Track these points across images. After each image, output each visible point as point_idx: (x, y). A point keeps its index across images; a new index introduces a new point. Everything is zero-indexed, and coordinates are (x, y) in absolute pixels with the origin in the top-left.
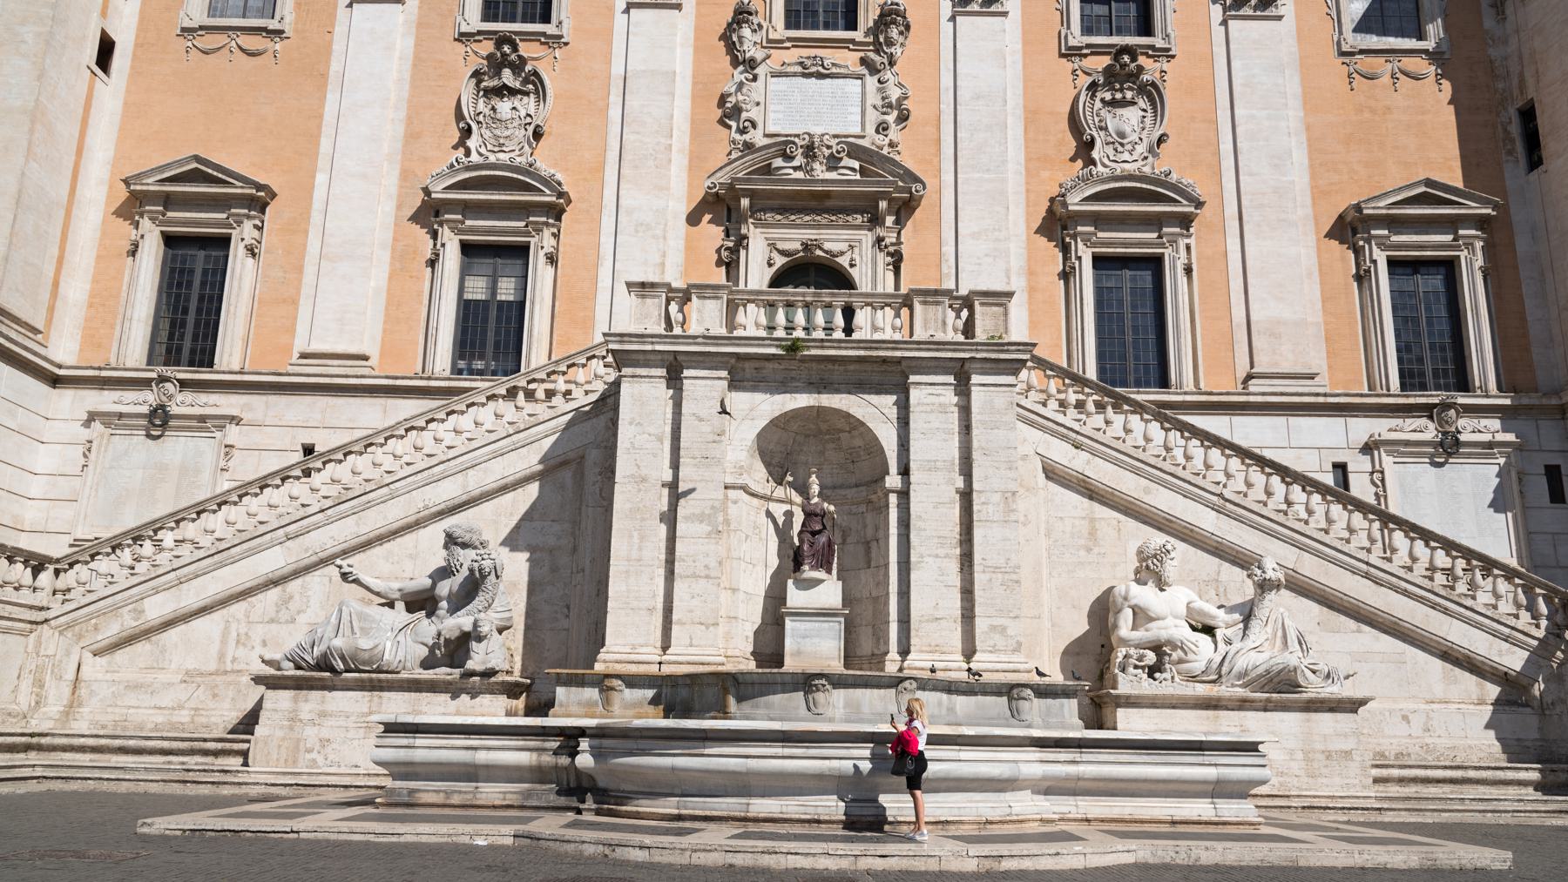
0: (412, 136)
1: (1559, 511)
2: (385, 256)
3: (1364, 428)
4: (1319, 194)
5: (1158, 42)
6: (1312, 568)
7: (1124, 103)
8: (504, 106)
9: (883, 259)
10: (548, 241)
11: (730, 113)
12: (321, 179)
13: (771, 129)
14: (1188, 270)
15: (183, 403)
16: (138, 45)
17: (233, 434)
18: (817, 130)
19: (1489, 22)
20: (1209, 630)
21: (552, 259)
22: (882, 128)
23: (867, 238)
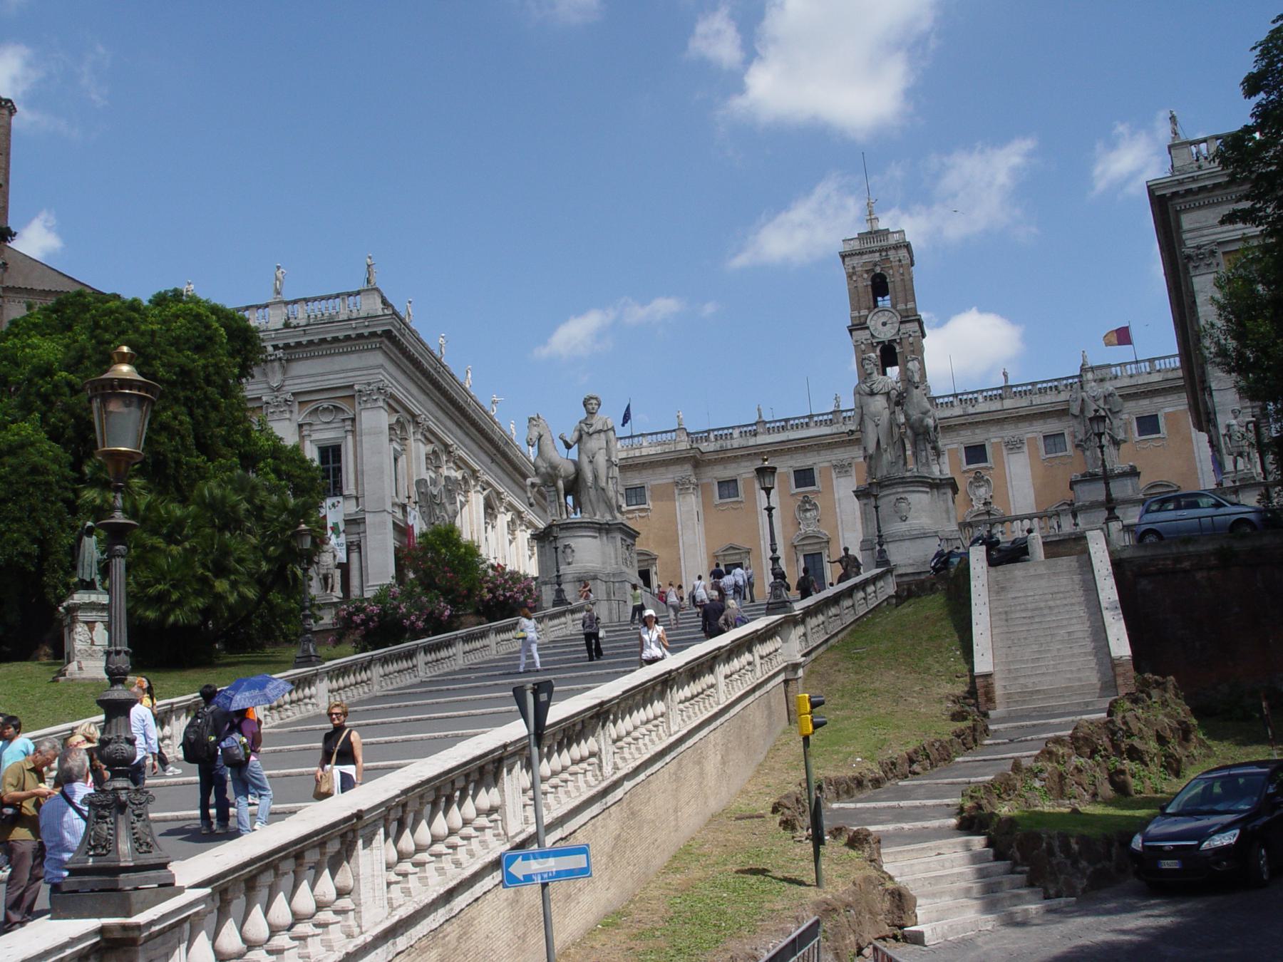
5: (988, 465)
8: (808, 514)
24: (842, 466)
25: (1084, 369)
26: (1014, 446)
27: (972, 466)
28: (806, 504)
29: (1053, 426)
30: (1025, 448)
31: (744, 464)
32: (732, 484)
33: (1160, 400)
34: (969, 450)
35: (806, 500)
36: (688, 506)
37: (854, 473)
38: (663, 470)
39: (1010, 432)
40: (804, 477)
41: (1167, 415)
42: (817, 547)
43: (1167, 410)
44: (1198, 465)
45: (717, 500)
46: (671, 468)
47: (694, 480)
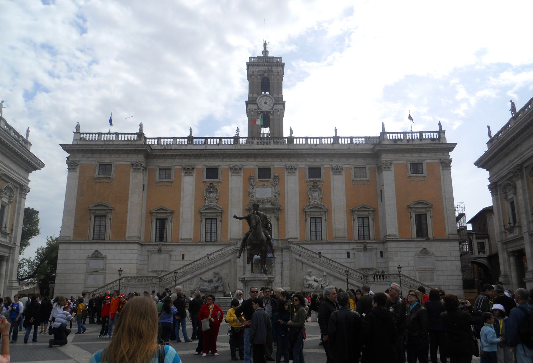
0: (196, 199)
1: (382, 259)
2: (193, 221)
3: (352, 246)
4: (347, 206)
5: (321, 180)
6: (332, 273)
7: (315, 191)
8: (211, 195)
9: (275, 219)
10: (220, 218)
11: (249, 193)
12: (181, 208)
13: (257, 197)
14: (325, 220)
15: (163, 248)
16: (148, 185)
17: (171, 253)
18: (264, 197)
19: (377, 174)
20: (317, 282)
21: (221, 221)
22: (275, 196)
23: (273, 216)
24: (236, 169)
25: (384, 133)
26: (337, 171)
27: (312, 179)
28: (211, 189)
29: (361, 162)
30: (343, 173)
31: (177, 160)
32: (167, 171)
33: (424, 155)
34: (311, 169)
35: (211, 186)
36: (137, 180)
37: (242, 174)
38: (125, 156)
39: (336, 163)
40: (212, 172)
41: (428, 164)
42: (215, 215)
43: (428, 161)
44: (443, 194)
45: (157, 179)
46: (131, 156)
47: (144, 164)
